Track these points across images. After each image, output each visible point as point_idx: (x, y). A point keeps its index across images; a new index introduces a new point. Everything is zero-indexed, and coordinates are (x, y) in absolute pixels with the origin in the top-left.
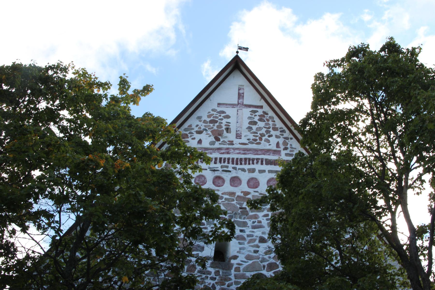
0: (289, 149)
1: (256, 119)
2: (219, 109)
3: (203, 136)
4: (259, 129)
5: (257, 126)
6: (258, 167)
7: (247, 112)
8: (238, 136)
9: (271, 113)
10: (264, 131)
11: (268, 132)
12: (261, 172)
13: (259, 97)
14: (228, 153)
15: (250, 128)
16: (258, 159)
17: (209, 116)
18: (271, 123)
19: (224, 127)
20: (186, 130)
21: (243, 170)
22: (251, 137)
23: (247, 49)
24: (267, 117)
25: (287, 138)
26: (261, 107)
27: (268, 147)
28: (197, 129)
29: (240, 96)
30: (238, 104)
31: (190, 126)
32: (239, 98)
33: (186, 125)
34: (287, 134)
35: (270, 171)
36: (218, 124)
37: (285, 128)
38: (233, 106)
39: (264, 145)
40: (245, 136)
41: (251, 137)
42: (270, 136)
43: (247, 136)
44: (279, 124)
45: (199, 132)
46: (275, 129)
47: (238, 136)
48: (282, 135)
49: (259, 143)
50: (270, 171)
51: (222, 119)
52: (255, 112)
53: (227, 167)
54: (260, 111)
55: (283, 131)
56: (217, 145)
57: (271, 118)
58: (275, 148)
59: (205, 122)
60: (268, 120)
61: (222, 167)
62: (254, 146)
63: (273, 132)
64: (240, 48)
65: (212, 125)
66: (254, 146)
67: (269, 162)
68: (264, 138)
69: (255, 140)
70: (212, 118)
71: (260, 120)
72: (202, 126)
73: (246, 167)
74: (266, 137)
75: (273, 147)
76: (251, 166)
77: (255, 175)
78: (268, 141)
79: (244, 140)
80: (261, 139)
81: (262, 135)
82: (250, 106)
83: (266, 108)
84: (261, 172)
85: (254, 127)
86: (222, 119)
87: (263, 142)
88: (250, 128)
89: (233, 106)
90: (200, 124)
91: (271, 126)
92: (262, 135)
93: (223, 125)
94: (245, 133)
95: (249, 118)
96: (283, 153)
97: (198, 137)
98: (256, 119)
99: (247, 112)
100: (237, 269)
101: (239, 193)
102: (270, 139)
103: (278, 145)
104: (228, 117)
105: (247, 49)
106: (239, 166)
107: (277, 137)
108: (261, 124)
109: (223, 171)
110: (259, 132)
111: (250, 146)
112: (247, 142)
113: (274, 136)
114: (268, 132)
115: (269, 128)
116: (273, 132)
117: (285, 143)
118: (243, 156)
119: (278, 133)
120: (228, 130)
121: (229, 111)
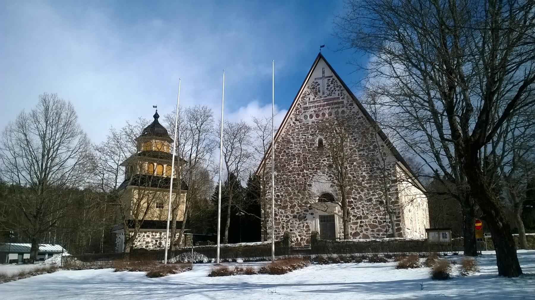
0: (343, 95)
2: (315, 81)
4: (331, 88)
5: (330, 87)
7: (326, 80)
9: (336, 79)
13: (331, 71)
14: (320, 102)
15: (327, 89)
16: (331, 103)
17: (312, 86)
19: (318, 90)
22: (328, 93)
23: (323, 46)
24: (334, 81)
25: (342, 90)
26: (332, 76)
28: (308, 93)
29: (323, 72)
30: (323, 77)
31: (305, 92)
32: (323, 74)
34: (342, 88)
36: (315, 89)
37: (341, 85)
38: (321, 78)
40: (326, 93)
42: (335, 91)
44: (339, 84)
45: (309, 94)
46: (337, 87)
47: (323, 93)
48: (340, 89)
49: (331, 95)
51: (316, 86)
52: (330, 79)
53: (320, 109)
55: (341, 87)
56: (316, 100)
57: (336, 81)
58: (337, 97)
60: (335, 83)
61: (318, 109)
64: (321, 47)
65: (313, 90)
68: (333, 92)
69: (330, 94)
70: (313, 87)
71: (332, 83)
74: (334, 91)
75: (337, 96)
78: (334, 93)
79: (325, 95)
80: (332, 93)
81: (333, 91)
82: (327, 77)
83: (334, 77)
85: (329, 88)
86: (316, 86)
87: (333, 94)
89: (321, 78)
91: (336, 85)
92: (333, 91)
93: (317, 89)
94: (326, 91)
95: (327, 83)
96: (341, 98)
98: (330, 84)
99: (326, 80)
102: (335, 92)
103: (339, 95)
104: (319, 85)
105: (323, 46)
107: (338, 90)
108: (332, 85)
109: (319, 111)
110: (331, 90)
111: (328, 97)
112: (327, 95)
113: (337, 91)
114: (335, 89)
115: (335, 87)
116: (337, 89)
117: (341, 93)
119: (338, 88)
120: (319, 91)
121: (320, 81)
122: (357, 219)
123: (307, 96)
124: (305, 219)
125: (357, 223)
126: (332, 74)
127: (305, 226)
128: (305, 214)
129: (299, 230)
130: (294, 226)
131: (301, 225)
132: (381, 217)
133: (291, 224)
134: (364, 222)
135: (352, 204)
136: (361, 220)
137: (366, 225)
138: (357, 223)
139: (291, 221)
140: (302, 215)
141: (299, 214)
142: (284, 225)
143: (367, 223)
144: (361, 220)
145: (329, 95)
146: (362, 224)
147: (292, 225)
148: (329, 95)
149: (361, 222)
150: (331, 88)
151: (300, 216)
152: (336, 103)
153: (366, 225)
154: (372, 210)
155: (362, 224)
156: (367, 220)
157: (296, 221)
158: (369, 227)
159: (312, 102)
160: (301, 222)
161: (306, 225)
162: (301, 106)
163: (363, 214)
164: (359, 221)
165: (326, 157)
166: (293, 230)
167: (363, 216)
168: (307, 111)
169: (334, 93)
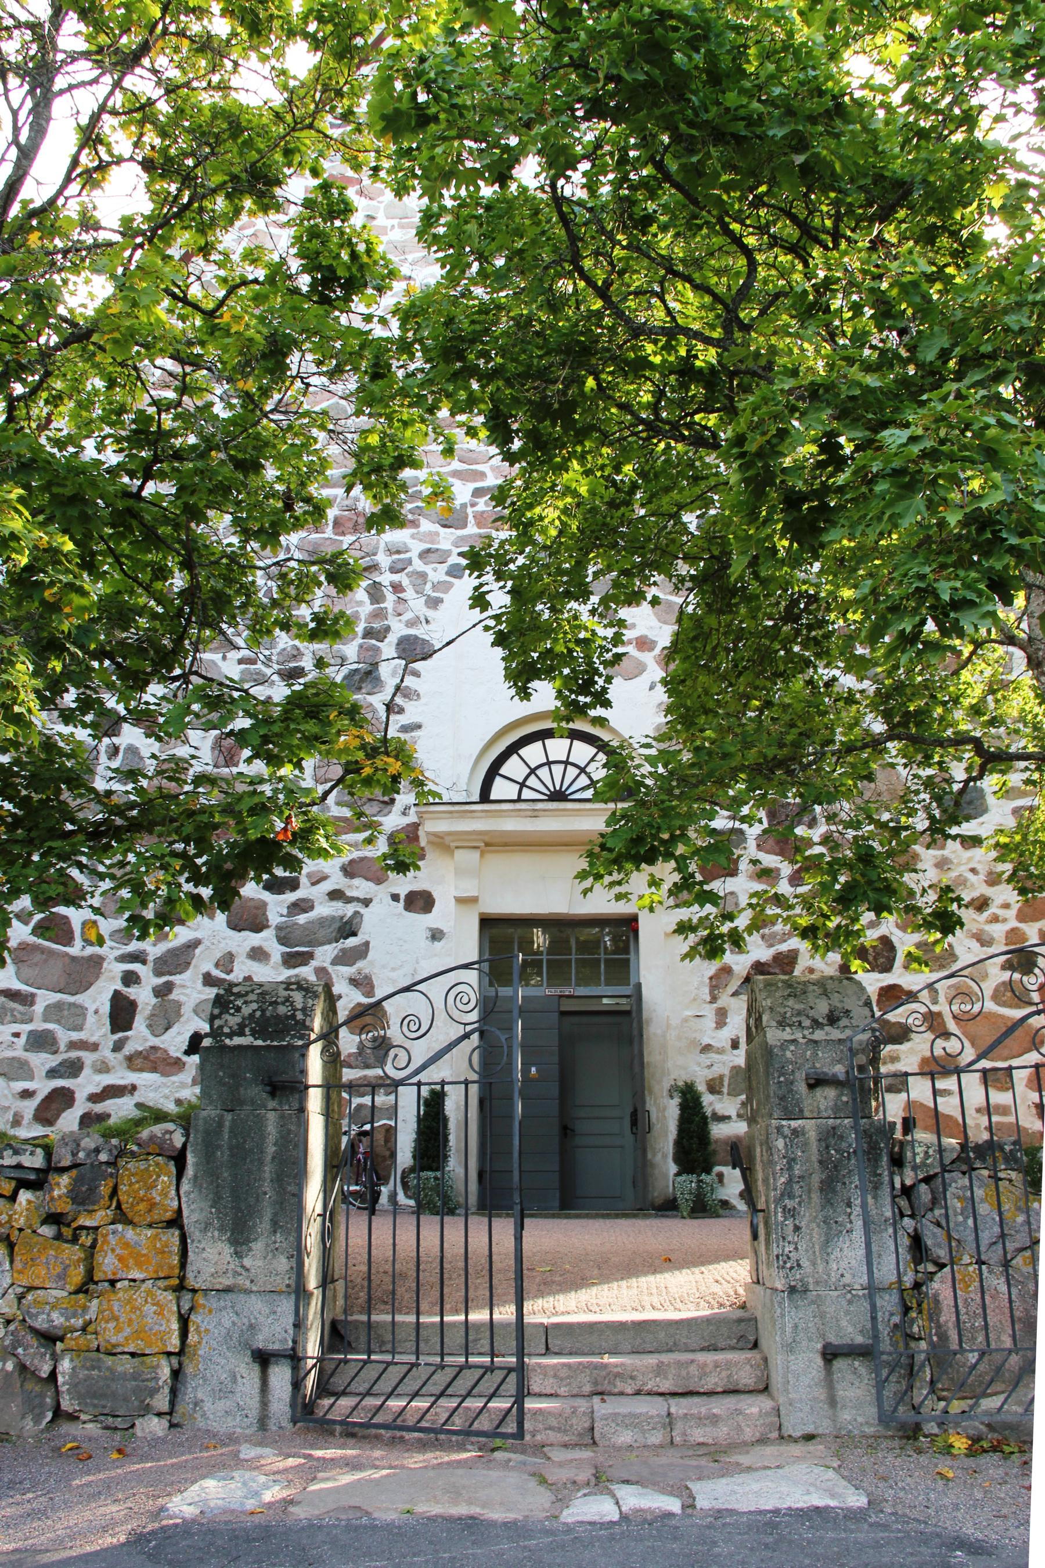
124: (352, 942)
128: (350, 900)
134: (912, 996)
135: (800, 831)
137: (933, 1022)
139: (204, 963)
140: (324, 909)
141: (291, 897)
142: (132, 992)
143: (942, 1007)
151: (302, 919)
153: (933, 1022)
154: (989, 891)
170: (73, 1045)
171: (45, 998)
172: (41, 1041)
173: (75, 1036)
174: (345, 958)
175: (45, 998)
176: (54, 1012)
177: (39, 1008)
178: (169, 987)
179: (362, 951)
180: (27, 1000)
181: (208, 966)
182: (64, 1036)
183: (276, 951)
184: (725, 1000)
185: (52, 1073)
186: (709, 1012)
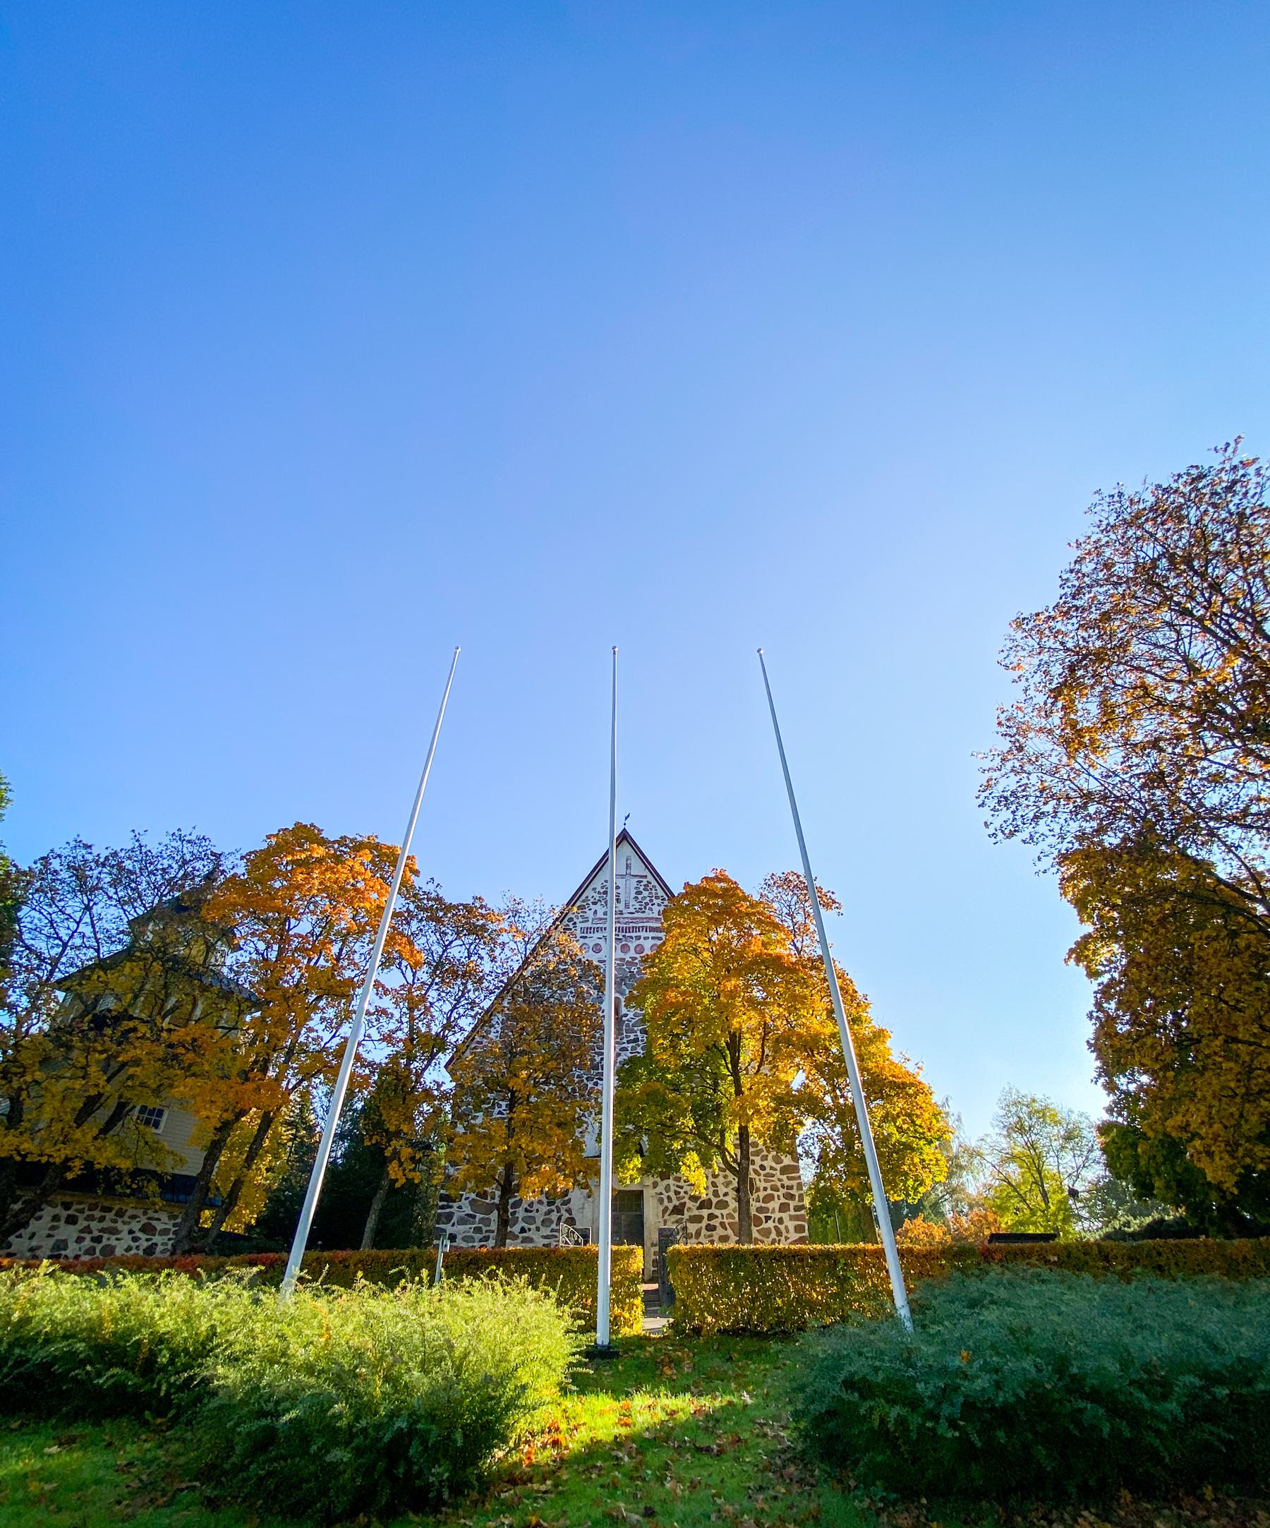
1: (642, 888)
3: (597, 907)
4: (645, 898)
6: (643, 934)
8: (627, 906)
9: (654, 883)
10: (647, 900)
11: (651, 901)
12: (646, 938)
15: (636, 898)
17: (602, 888)
18: (653, 891)
20: (583, 901)
21: (631, 937)
22: (637, 906)
24: (650, 886)
27: (651, 916)
28: (592, 900)
29: (628, 866)
33: (583, 897)
35: (653, 938)
39: (648, 914)
41: (637, 906)
43: (634, 905)
44: (661, 893)
45: (595, 903)
46: (657, 898)
47: (627, 906)
50: (653, 938)
52: (642, 882)
54: (645, 882)
59: (599, 893)
62: (640, 915)
63: (655, 901)
66: (640, 915)
67: (653, 929)
72: (597, 896)
73: (634, 935)
76: (638, 934)
77: (641, 941)
78: (651, 909)
79: (632, 910)
83: (650, 878)
84: (646, 938)
85: (640, 897)
88: (636, 898)
90: (595, 895)
94: (632, 902)
97: (593, 907)
100: (628, 1025)
101: (628, 959)
106: (628, 934)
107: (659, 905)
108: (646, 893)
111: (636, 915)
114: (651, 901)
116: (655, 901)
118: (631, 925)
119: (659, 901)
122: (699, 1208)
123: (592, 906)
125: (698, 1219)
126: (647, 873)
127: (563, 1219)
129: (545, 1231)
130: (534, 1218)
131: (554, 1216)
132: (758, 1205)
133: (526, 1210)
134: (717, 1217)
136: (710, 1211)
137: (722, 1224)
138: (698, 1219)
143: (725, 1220)
144: (710, 1211)
145: (640, 910)
146: (714, 1222)
147: (529, 1214)
148: (640, 910)
149: (711, 1217)
150: (645, 898)
152: (653, 929)
153: (722, 1224)
155: (714, 1222)
156: (725, 1212)
157: (540, 1202)
158: (730, 1232)
159: (601, 919)
160: (553, 1207)
161: (568, 1215)
162: (575, 923)
163: (716, 1194)
164: (705, 1212)
165: (628, 1042)
166: (530, 1230)
167: (715, 1200)
168: (589, 935)
169: (651, 909)
170: (487, 1231)
171: (479, 1216)
172: (478, 1230)
173: (488, 1228)
174: (564, 1203)
175: (479, 1216)
176: (482, 1220)
177: (477, 1220)
178: (515, 1212)
179: (569, 1201)
180: (474, 1217)
181: (526, 1206)
182: (484, 1229)
183: (545, 1201)
184: (666, 1217)
185: (481, 1240)
186: (661, 1220)
